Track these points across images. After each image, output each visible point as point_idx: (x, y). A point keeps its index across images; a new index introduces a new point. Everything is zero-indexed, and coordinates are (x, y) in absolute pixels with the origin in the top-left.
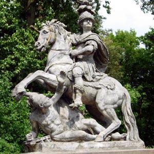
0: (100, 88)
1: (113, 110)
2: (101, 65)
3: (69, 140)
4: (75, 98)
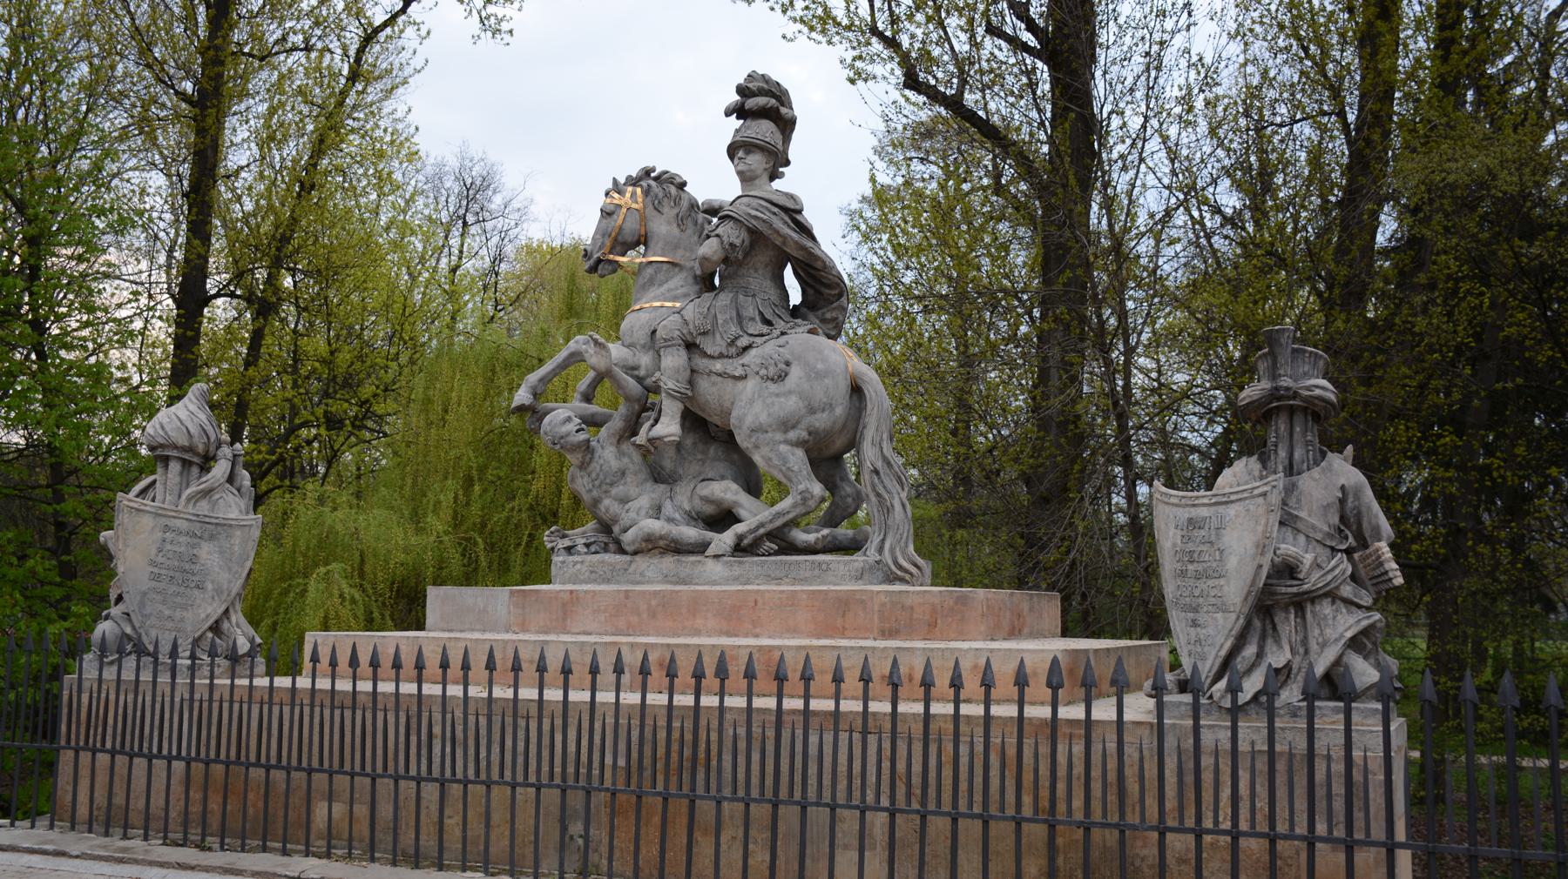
0: (743, 378)
1: (783, 448)
2: (821, 293)
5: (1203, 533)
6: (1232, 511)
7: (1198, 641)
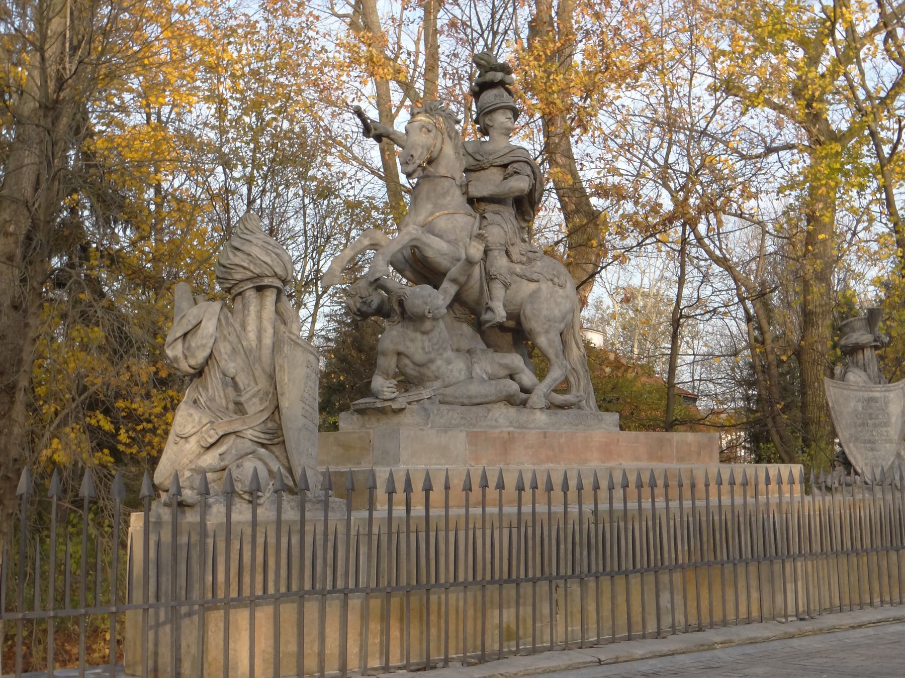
0: (537, 281)
3: (478, 400)
4: (491, 299)
5: (877, 404)
6: (892, 395)
7: (875, 458)
